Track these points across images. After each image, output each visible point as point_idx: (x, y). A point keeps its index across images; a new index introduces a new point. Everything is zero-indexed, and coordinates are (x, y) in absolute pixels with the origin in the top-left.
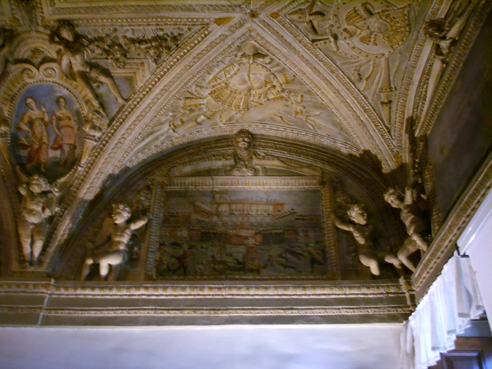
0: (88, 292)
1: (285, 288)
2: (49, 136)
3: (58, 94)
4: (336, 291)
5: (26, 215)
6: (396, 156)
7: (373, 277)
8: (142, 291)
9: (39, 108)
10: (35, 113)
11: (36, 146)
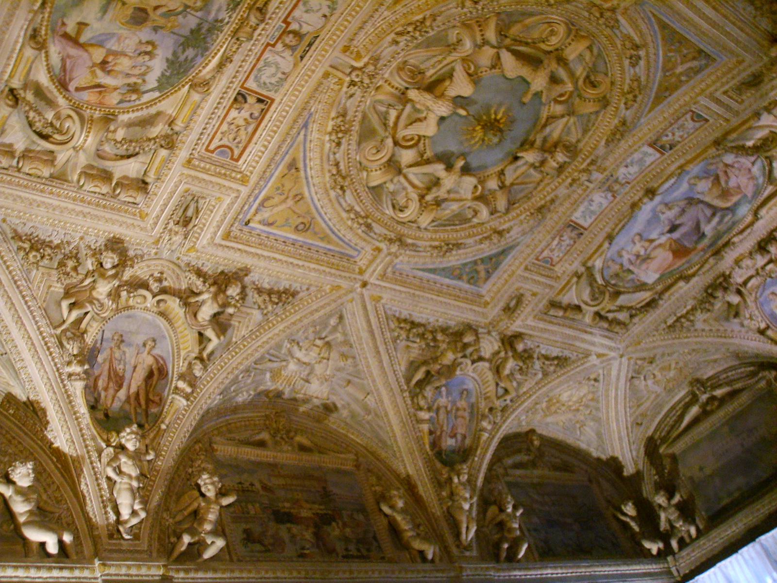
0: (517, 573)
1: (618, 565)
2: (448, 425)
3: (465, 387)
4: (642, 567)
5: (463, 503)
6: (636, 464)
7: (652, 556)
8: (549, 571)
9: (447, 397)
10: (443, 401)
11: (438, 433)
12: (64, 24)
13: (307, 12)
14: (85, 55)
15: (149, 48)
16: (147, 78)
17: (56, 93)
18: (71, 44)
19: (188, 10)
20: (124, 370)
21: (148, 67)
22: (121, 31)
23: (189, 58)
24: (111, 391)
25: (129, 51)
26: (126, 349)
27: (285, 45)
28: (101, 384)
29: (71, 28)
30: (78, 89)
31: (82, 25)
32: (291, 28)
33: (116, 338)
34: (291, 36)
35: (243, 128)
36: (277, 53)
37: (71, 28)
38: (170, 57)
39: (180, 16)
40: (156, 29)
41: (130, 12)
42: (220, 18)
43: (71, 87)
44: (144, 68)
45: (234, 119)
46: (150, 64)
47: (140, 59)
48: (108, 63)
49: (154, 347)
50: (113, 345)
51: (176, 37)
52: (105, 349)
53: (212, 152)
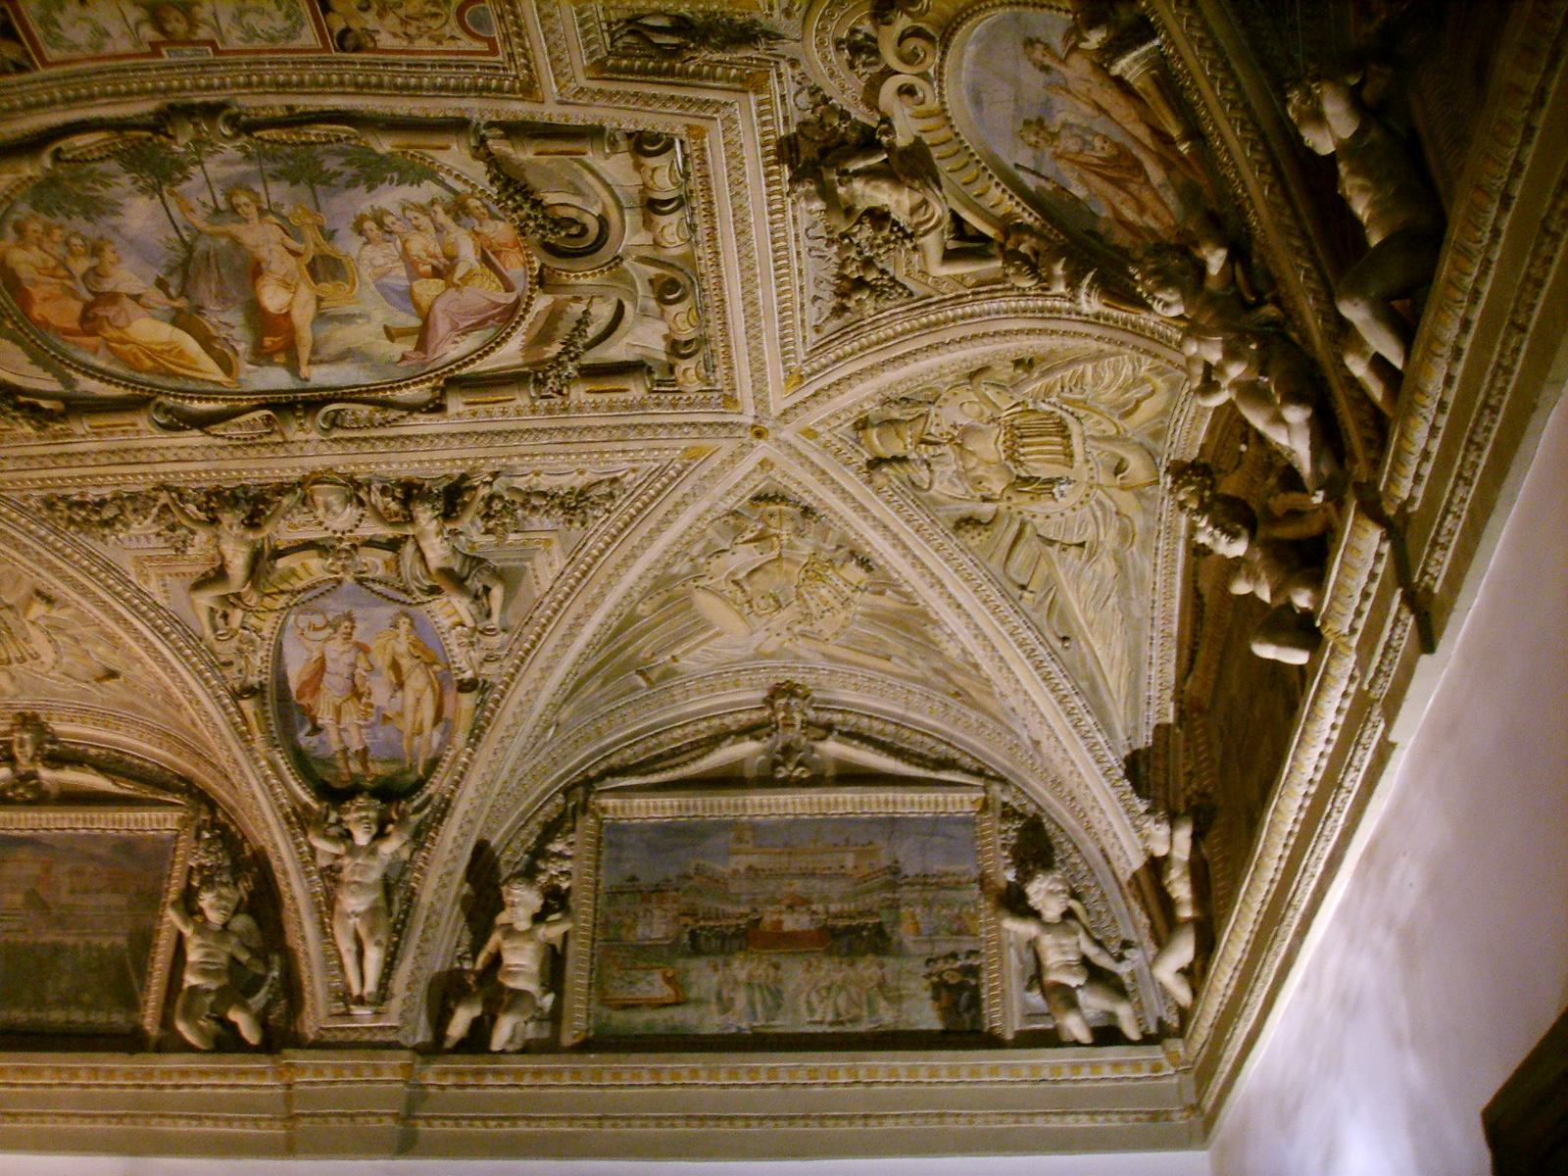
12: (404, 357)
13: (107, 34)
14: (439, 306)
15: (369, 225)
16: (424, 201)
17: (529, 318)
18: (431, 334)
19: (266, 207)
20: (1105, 139)
21: (404, 209)
22: (369, 280)
23: (342, 160)
24: (1146, 196)
25: (394, 249)
26: (1060, 117)
27: (193, 24)
28: (1129, 214)
29: (406, 346)
30: (509, 288)
31: (391, 334)
32: (159, 37)
33: (1033, 139)
34: (169, 27)
35: (402, 12)
36: (218, 30)
37: (406, 346)
38: (363, 188)
39: (284, 212)
40: (330, 236)
41: (327, 287)
42: (240, 154)
43: (512, 298)
44: (410, 214)
45: (395, 35)
46: (396, 210)
47: (396, 228)
48: (434, 268)
49: (1047, 47)
50: (1049, 151)
51: (322, 202)
52: (1057, 172)
53: (491, 42)
